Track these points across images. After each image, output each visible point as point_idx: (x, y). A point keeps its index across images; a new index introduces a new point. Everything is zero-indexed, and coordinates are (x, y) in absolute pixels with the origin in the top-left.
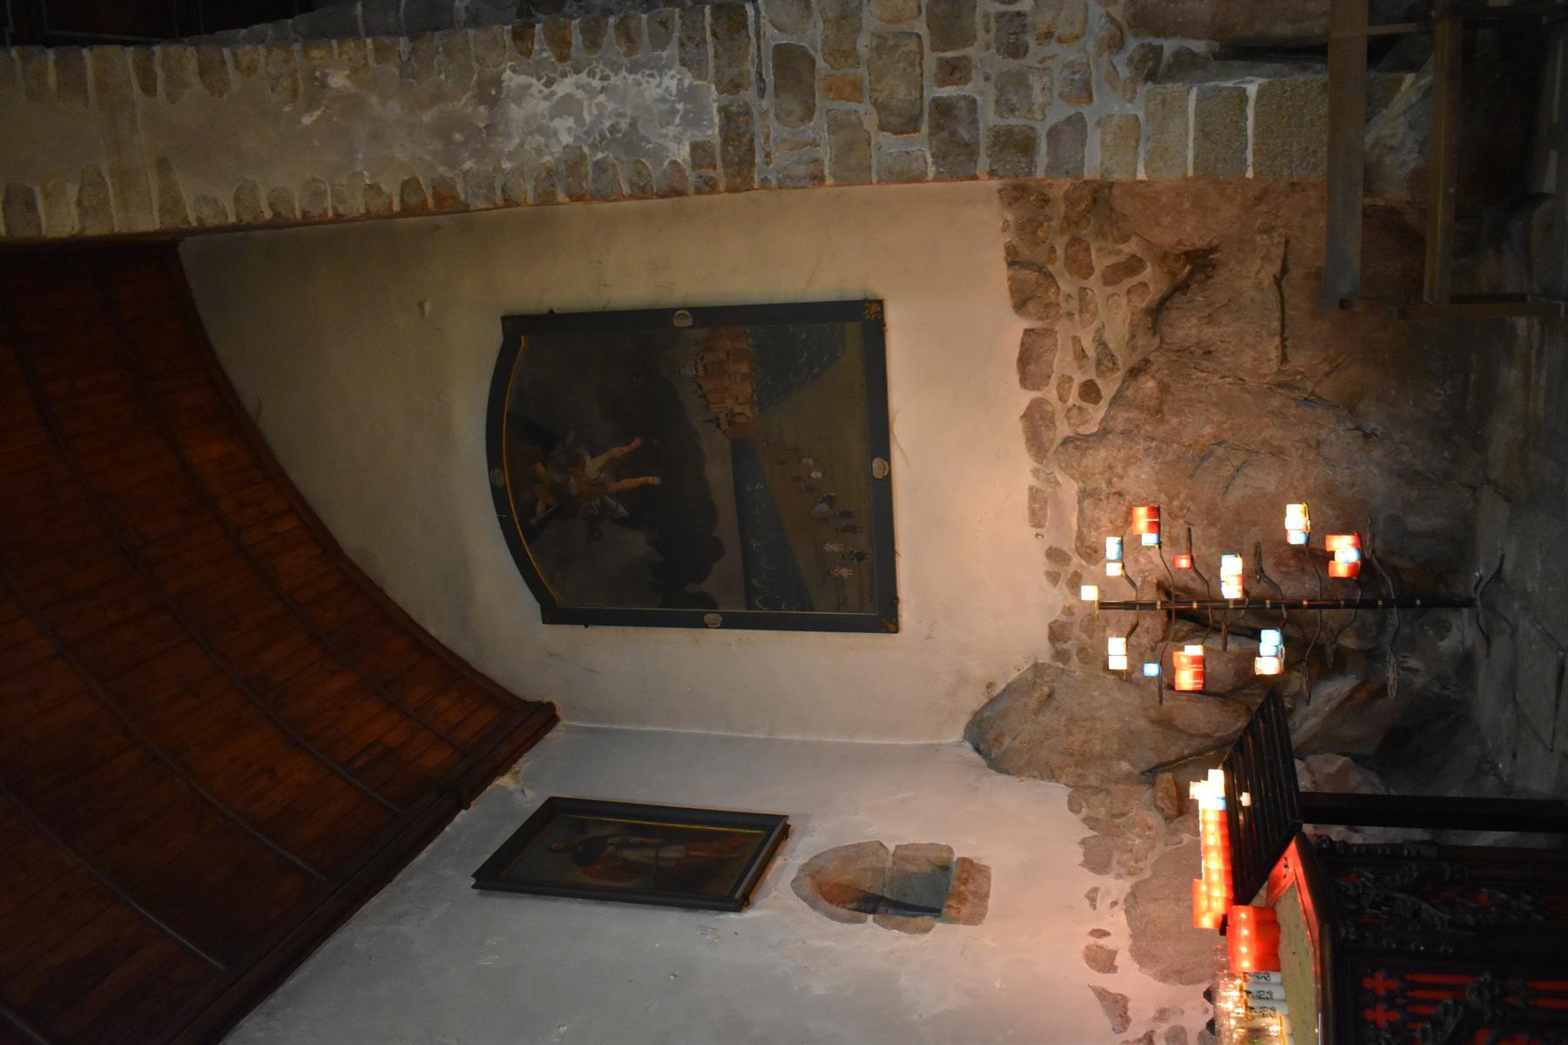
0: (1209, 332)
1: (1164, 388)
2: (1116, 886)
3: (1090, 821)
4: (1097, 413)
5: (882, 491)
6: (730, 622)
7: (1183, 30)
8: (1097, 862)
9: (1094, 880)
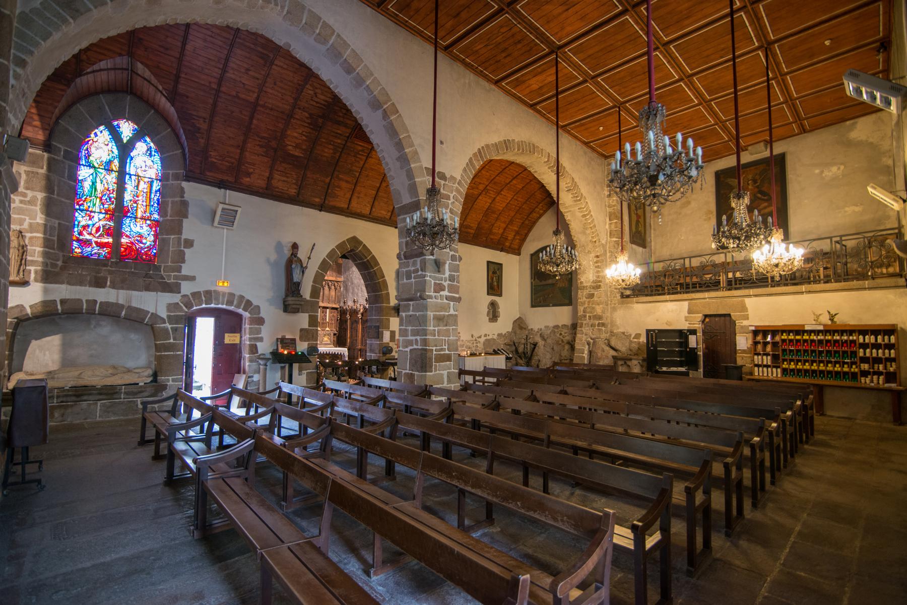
0: (566, 350)
1: (560, 344)
2: (495, 337)
3: (505, 334)
4: (558, 335)
5: (548, 306)
6: (532, 283)
7: (593, 347)
8: (499, 335)
9: (496, 334)
